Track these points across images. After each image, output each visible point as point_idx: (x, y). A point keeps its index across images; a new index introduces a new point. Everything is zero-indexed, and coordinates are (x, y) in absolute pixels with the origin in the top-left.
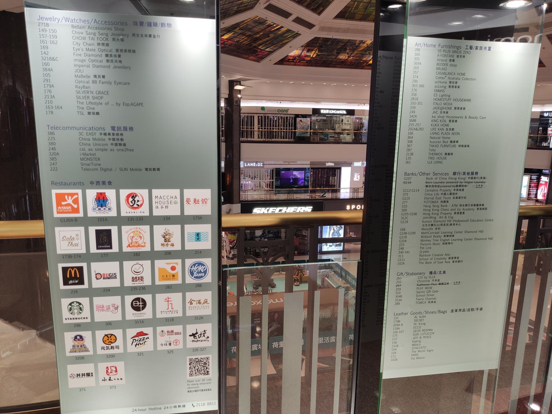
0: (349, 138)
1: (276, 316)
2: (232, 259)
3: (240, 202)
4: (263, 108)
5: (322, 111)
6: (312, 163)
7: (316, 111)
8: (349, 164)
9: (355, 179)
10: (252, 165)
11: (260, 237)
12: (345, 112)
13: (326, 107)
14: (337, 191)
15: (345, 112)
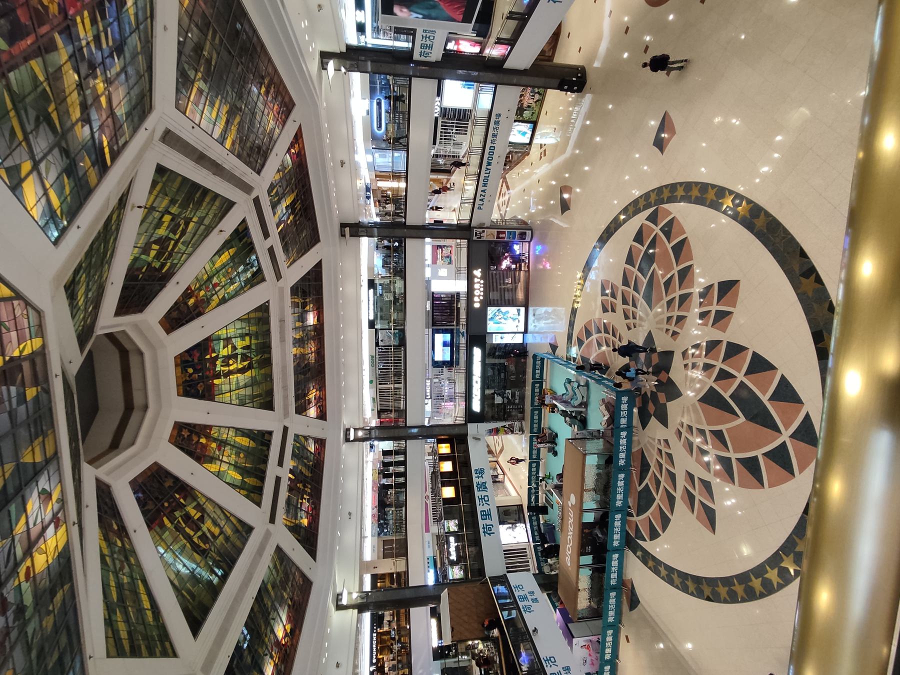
0: (399, 284)
1: (586, 531)
2: (523, 432)
3: (466, 424)
4: (371, 382)
5: (372, 318)
6: (427, 327)
7: (372, 325)
8: (428, 282)
9: (446, 275)
10: (428, 391)
11: (503, 398)
12: (372, 291)
13: (367, 312)
14: (458, 294)
15: (372, 291)
